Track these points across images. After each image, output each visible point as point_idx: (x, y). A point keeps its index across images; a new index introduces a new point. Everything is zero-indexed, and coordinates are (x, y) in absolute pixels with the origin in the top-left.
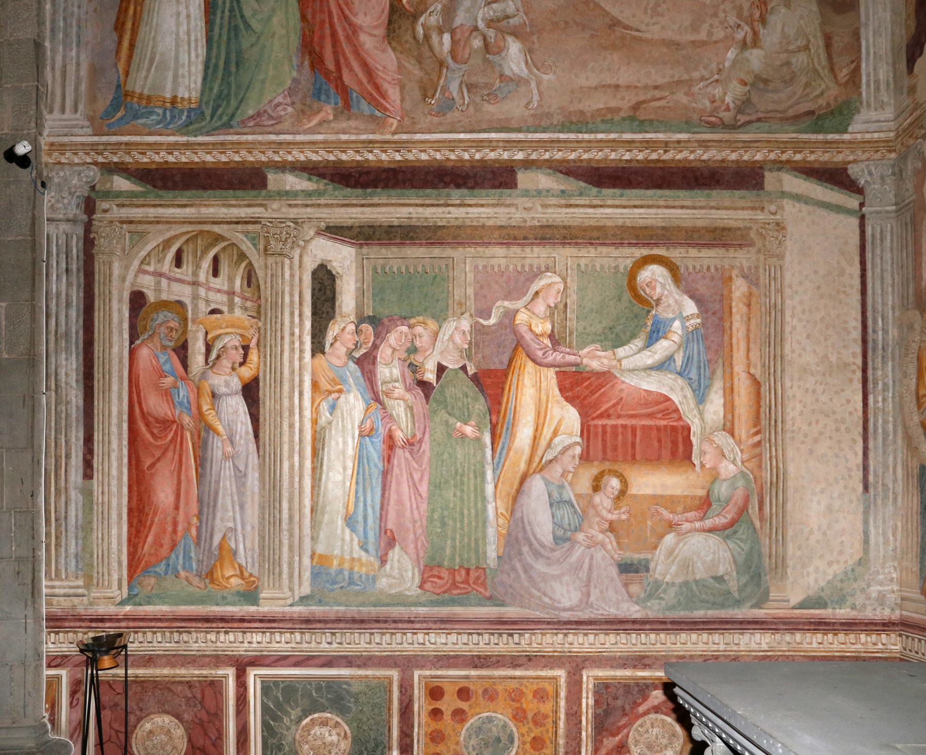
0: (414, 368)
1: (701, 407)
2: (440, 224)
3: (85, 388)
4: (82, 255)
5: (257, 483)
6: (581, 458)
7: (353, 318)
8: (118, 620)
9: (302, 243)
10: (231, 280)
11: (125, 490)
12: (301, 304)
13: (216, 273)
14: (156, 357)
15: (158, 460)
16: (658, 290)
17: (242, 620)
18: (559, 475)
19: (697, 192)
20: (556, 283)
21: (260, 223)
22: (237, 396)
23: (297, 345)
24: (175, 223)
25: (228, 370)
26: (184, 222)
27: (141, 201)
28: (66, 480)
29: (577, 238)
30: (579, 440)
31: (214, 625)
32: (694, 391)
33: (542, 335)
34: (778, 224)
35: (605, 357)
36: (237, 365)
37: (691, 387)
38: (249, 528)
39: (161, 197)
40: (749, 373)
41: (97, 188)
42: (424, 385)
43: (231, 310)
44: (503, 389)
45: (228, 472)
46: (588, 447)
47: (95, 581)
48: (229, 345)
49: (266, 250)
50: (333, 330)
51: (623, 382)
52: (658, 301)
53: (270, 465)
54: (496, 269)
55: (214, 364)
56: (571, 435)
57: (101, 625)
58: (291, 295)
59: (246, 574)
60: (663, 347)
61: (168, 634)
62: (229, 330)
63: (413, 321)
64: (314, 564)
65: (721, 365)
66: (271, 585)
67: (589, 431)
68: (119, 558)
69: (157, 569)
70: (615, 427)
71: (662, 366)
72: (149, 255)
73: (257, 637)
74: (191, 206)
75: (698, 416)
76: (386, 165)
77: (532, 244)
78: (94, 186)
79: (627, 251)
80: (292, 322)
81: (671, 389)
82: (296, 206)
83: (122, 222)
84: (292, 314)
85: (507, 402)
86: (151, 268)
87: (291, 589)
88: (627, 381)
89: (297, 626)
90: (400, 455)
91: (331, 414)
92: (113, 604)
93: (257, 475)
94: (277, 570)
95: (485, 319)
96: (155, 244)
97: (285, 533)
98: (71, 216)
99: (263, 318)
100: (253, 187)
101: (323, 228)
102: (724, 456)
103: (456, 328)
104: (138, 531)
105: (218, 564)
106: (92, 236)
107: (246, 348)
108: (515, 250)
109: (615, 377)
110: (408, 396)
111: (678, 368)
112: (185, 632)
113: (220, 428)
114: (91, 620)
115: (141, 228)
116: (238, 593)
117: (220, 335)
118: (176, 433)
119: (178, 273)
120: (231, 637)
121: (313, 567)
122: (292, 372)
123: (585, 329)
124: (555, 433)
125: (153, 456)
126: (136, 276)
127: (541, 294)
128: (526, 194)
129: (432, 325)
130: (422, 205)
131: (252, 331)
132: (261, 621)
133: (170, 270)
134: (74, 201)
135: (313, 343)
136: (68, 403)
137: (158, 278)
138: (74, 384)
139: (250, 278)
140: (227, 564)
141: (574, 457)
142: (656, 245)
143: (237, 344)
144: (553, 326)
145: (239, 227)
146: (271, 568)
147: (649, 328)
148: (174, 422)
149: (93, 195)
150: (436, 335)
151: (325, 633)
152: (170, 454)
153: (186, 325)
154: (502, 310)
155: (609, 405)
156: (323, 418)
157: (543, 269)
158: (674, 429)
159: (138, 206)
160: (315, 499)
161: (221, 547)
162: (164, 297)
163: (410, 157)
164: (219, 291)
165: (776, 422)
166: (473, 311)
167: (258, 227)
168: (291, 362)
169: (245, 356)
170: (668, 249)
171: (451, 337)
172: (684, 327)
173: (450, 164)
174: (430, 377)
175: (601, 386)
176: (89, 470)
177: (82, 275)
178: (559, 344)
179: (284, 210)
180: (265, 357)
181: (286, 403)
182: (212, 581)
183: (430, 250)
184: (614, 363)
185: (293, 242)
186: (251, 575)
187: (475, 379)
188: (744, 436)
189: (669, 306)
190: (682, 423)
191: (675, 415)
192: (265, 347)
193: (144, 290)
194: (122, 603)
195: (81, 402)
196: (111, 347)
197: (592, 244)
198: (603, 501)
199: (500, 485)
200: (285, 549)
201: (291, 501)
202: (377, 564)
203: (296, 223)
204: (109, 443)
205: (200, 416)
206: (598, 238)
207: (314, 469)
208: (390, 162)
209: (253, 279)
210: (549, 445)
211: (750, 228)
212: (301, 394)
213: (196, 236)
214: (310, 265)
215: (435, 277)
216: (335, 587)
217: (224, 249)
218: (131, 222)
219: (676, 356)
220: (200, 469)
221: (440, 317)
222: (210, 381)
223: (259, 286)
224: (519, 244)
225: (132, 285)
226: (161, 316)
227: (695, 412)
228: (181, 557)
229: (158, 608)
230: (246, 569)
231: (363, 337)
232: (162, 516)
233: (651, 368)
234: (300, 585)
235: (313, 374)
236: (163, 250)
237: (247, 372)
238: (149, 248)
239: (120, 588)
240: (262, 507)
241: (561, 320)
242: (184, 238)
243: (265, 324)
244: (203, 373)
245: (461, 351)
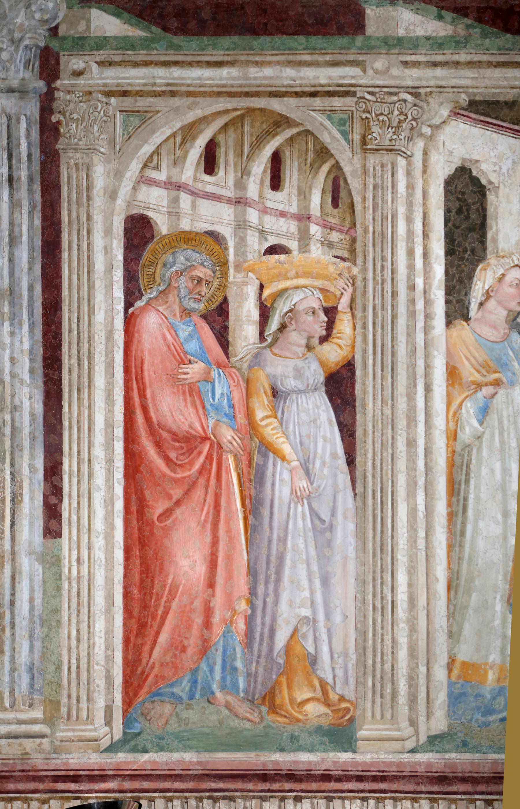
4: (36, 153)
5: (352, 540)
8: (104, 778)
9: (427, 130)
11: (119, 555)
12: (426, 235)
14: (173, 329)
15: (178, 503)
17: (326, 777)
21: (354, 94)
22: (316, 394)
23: (420, 305)
24: (203, 94)
25: (301, 350)
26: (219, 94)
27: (142, 55)
28: (13, 539)
31: (276, 786)
36: (315, 341)
38: (338, 618)
39: (178, 48)
41: (62, 31)
43: (304, 247)
45: (300, 523)
47: (64, 710)
48: (301, 308)
49: (364, 142)
53: (374, 510)
55: (275, 340)
57: (73, 786)
58: (409, 220)
59: (333, 697)
61: (193, 803)
62: (301, 281)
64: (454, 678)
66: (378, 716)
68: (108, 671)
69: (175, 690)
72: (157, 151)
74: (232, 64)
78: (56, 28)
80: (411, 267)
82: (416, 64)
83: (109, 94)
84: (411, 253)
86: (162, 176)
87: (413, 723)
89: (423, 788)
91: (481, 423)
92: (97, 750)
93: (351, 527)
94: (388, 689)
96: (168, 132)
97: (402, 625)
98: (15, 83)
99: (359, 260)
100: (341, 31)
101: (465, 104)
104: (142, 626)
105: (284, 679)
106: (54, 119)
112: (224, 798)
114: (57, 779)
115: (142, 103)
116: (319, 730)
117: (285, 290)
118: (209, 458)
121: (450, 684)
122: (412, 352)
125: (170, 497)
126: (134, 188)
131: (341, 283)
132: (359, 779)
133: (195, 179)
134: (20, 56)
135: (447, 302)
136: (15, 408)
137: (174, 193)
138: (26, 377)
140: (299, 678)
143: (316, 305)
145: (318, 102)
146: (378, 686)
149: (54, 45)
151: (473, 801)
152: (199, 493)
153: (225, 274)
156: (467, 429)
159: (136, 64)
160: (455, 567)
161: (288, 648)
162: (185, 225)
164: (283, 214)
167: (350, 101)
168: (410, 335)
169: (330, 326)
176: (53, 523)
177: (37, 187)
179: (395, 71)
180: (364, 326)
181: (402, 405)
182: (274, 709)
185: (412, 129)
186: (342, 698)
192: (364, 310)
193: (150, 214)
194: (112, 748)
195: (39, 408)
196: (91, 312)
200: (403, 654)
201: (411, 571)
203: (416, 95)
204: (90, 475)
207: (451, 516)
209: (343, 194)
212: (428, 389)
213: (242, 117)
216: (491, 718)
217: (291, 140)
218: (125, 94)
220: (251, 518)
222: (269, 370)
223: (352, 206)
225: (129, 204)
228: (218, 668)
229: (176, 756)
230: (334, 688)
232: (185, 600)
234: (429, 715)
235: (449, 355)
236: (183, 142)
238: (158, 138)
239: (109, 722)
240: (361, 582)
243: (364, 270)
244: (257, 356)
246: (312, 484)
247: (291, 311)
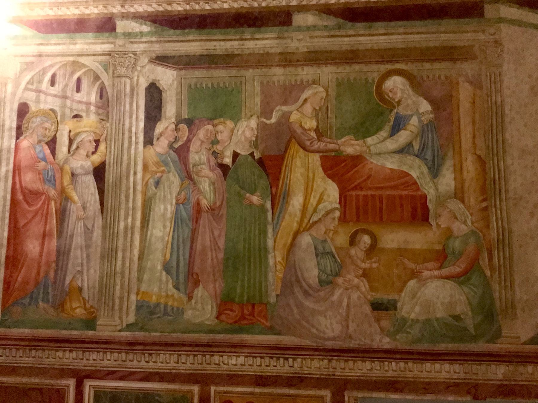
1: (435, 181)
2: (236, 53)
6: (339, 220)
7: (173, 120)
10: (89, 94)
12: (137, 111)
13: (78, 90)
16: (399, 94)
18: (323, 233)
19: (429, 21)
20: (320, 92)
22: (89, 175)
26: (58, 56)
29: (336, 59)
31: (62, 345)
32: (429, 168)
33: (310, 130)
34: (496, 42)
35: (358, 145)
36: (90, 153)
37: (427, 165)
38: (92, 271)
40: (475, 154)
42: (224, 168)
43: (88, 115)
44: (281, 169)
46: (345, 212)
49: (113, 73)
50: (160, 128)
51: (372, 163)
52: (399, 103)
53: (110, 224)
54: (276, 84)
56: (331, 203)
59: (88, 306)
60: (403, 137)
63: (216, 122)
65: (451, 149)
66: (106, 314)
67: (345, 200)
70: (365, 196)
71: (403, 150)
73: (94, 356)
75: (433, 187)
76: (199, 13)
77: (303, 65)
79: (375, 67)
81: (410, 167)
85: (284, 178)
86: (34, 87)
87: (120, 318)
88: (375, 162)
89: (123, 348)
90: (205, 219)
91: (156, 188)
94: (111, 304)
95: (267, 119)
97: (118, 275)
99: (110, 120)
101: (154, 58)
103: (246, 126)
105: (68, 298)
107: (97, 142)
108: (291, 69)
109: (366, 160)
110: (211, 175)
111: (416, 152)
112: (40, 349)
113: (76, 198)
118: (44, 203)
120: (74, 354)
121: (137, 300)
123: (342, 124)
124: (319, 202)
126: (23, 92)
127: (309, 101)
128: (299, 29)
129: (230, 124)
130: (224, 40)
132: (97, 343)
135: (145, 137)
137: (38, 94)
142: (397, 62)
144: (318, 123)
146: (107, 301)
147: (392, 123)
150: (232, 131)
151: (144, 354)
152: (38, 217)
154: (280, 112)
155: (361, 180)
157: (311, 82)
158: (413, 197)
163: (216, 6)
165: (500, 191)
166: (259, 114)
169: (96, 148)
170: (407, 64)
171: (244, 131)
172: (420, 121)
173: (244, 11)
174: (228, 160)
175: (355, 166)
178: (323, 136)
180: (111, 147)
183: (229, 71)
184: (365, 149)
187: (261, 162)
188: (472, 202)
189: (408, 105)
190: (419, 193)
191: (414, 187)
192: (111, 140)
197: (348, 63)
198: (357, 252)
200: (118, 288)
202: (185, 299)
203: (135, 54)
206: (352, 59)
208: (201, 10)
209: (104, 93)
210: (315, 211)
211: (473, 46)
214: (144, 84)
215: (232, 91)
216: (154, 317)
217: (85, 73)
219: (414, 143)
221: (236, 119)
224: (293, 66)
227: (431, 184)
228: (41, 292)
229: (21, 331)
230: (88, 302)
231: (180, 133)
233: (395, 152)
234: (127, 315)
237: (97, 159)
241: (324, 119)
243: (112, 124)
247: (81, 141)
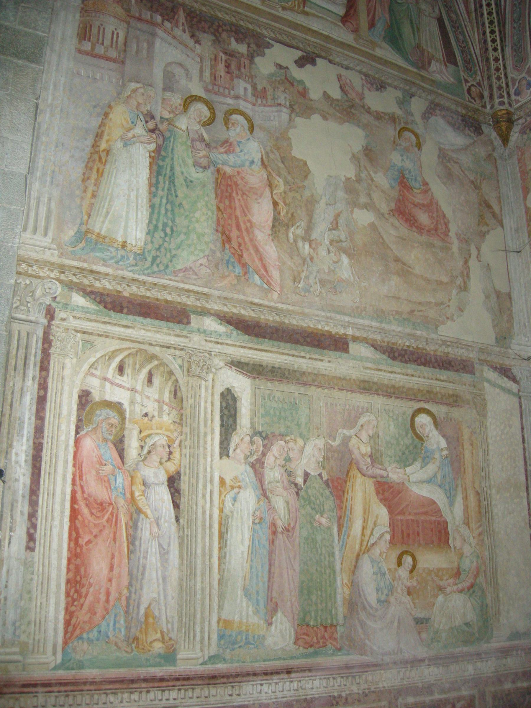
0: (290, 474)
3: (33, 469)
11: (65, 562)
18: (378, 554)
21: (185, 350)
25: (157, 464)
30: (388, 529)
43: (160, 416)
48: (158, 443)
49: (188, 371)
50: (235, 439)
55: (146, 458)
68: (56, 625)
100: (180, 322)
102: (465, 541)
117: (151, 434)
118: (112, 514)
119: (119, 380)
125: (92, 533)
133: (113, 377)
139: (175, 393)
141: (386, 542)
143: (165, 443)
148: (110, 504)
152: (106, 532)
156: (227, 508)
167: (183, 353)
193: (92, 391)
199: (344, 562)
203: (211, 355)
204: (52, 519)
205: (133, 500)
214: (219, 390)
217: (157, 366)
220: (130, 545)
222: (142, 472)
226: (103, 413)
231: (255, 446)
232: (97, 587)
236: (110, 358)
237: (172, 467)
239: (54, 653)
242: (126, 353)
244: (137, 465)
245: (319, 463)
246: (160, 530)
247: (153, 445)
